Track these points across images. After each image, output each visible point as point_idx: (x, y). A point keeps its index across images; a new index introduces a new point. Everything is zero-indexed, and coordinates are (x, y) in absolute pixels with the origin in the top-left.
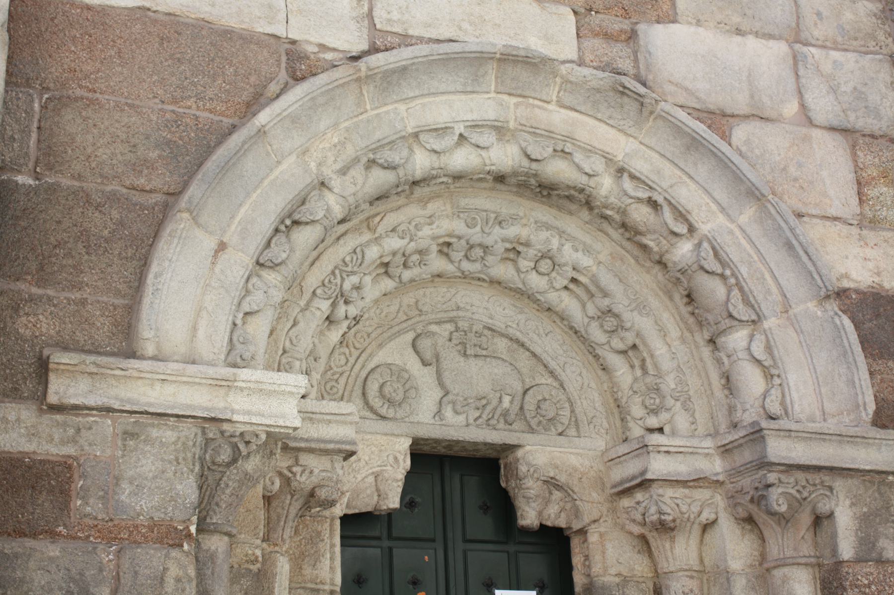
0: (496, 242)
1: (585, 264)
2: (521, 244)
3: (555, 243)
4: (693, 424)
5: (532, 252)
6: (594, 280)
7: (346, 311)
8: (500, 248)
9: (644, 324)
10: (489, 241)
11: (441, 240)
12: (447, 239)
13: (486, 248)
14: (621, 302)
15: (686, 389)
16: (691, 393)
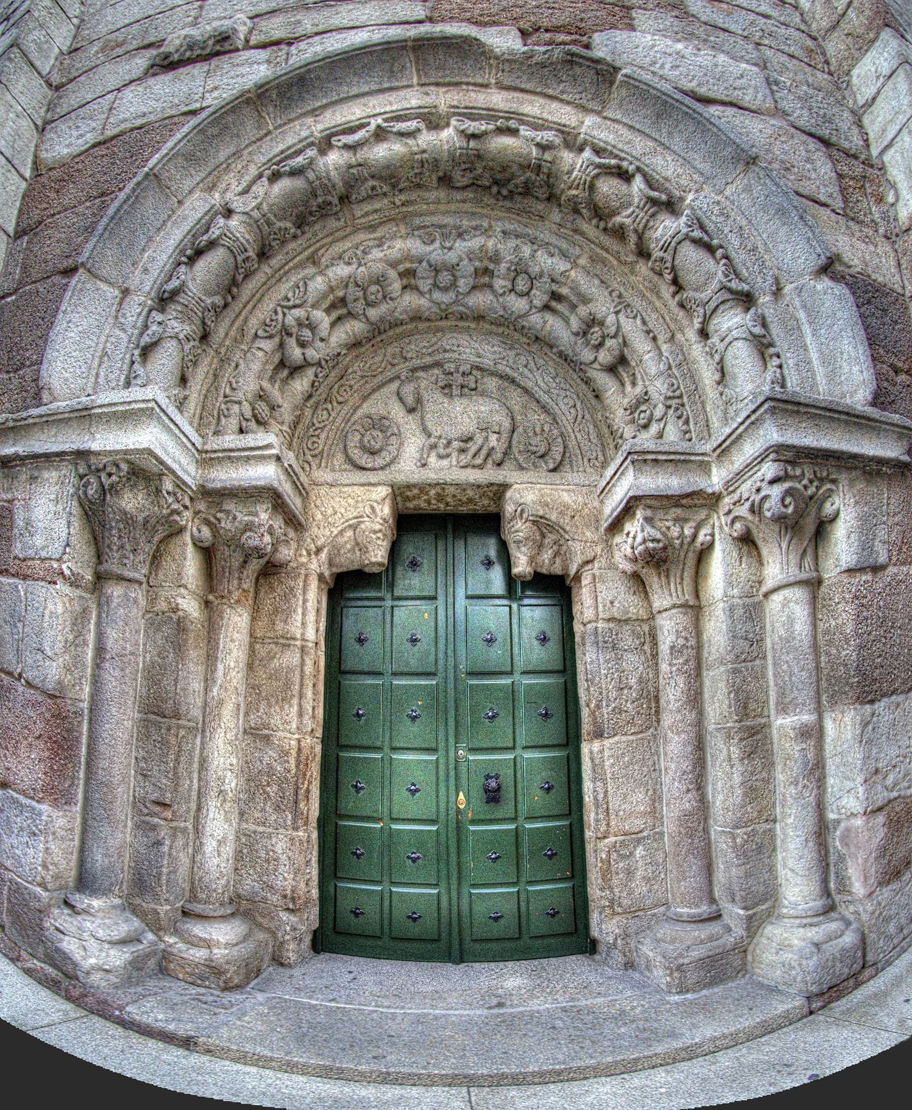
0: (461, 259)
1: (562, 269)
2: (490, 259)
3: (527, 250)
4: (686, 433)
5: (503, 266)
6: (574, 289)
7: (303, 354)
8: (467, 268)
9: (631, 328)
10: (451, 257)
11: (401, 268)
12: (408, 265)
13: (452, 269)
14: (603, 306)
15: (678, 393)
16: (685, 400)
